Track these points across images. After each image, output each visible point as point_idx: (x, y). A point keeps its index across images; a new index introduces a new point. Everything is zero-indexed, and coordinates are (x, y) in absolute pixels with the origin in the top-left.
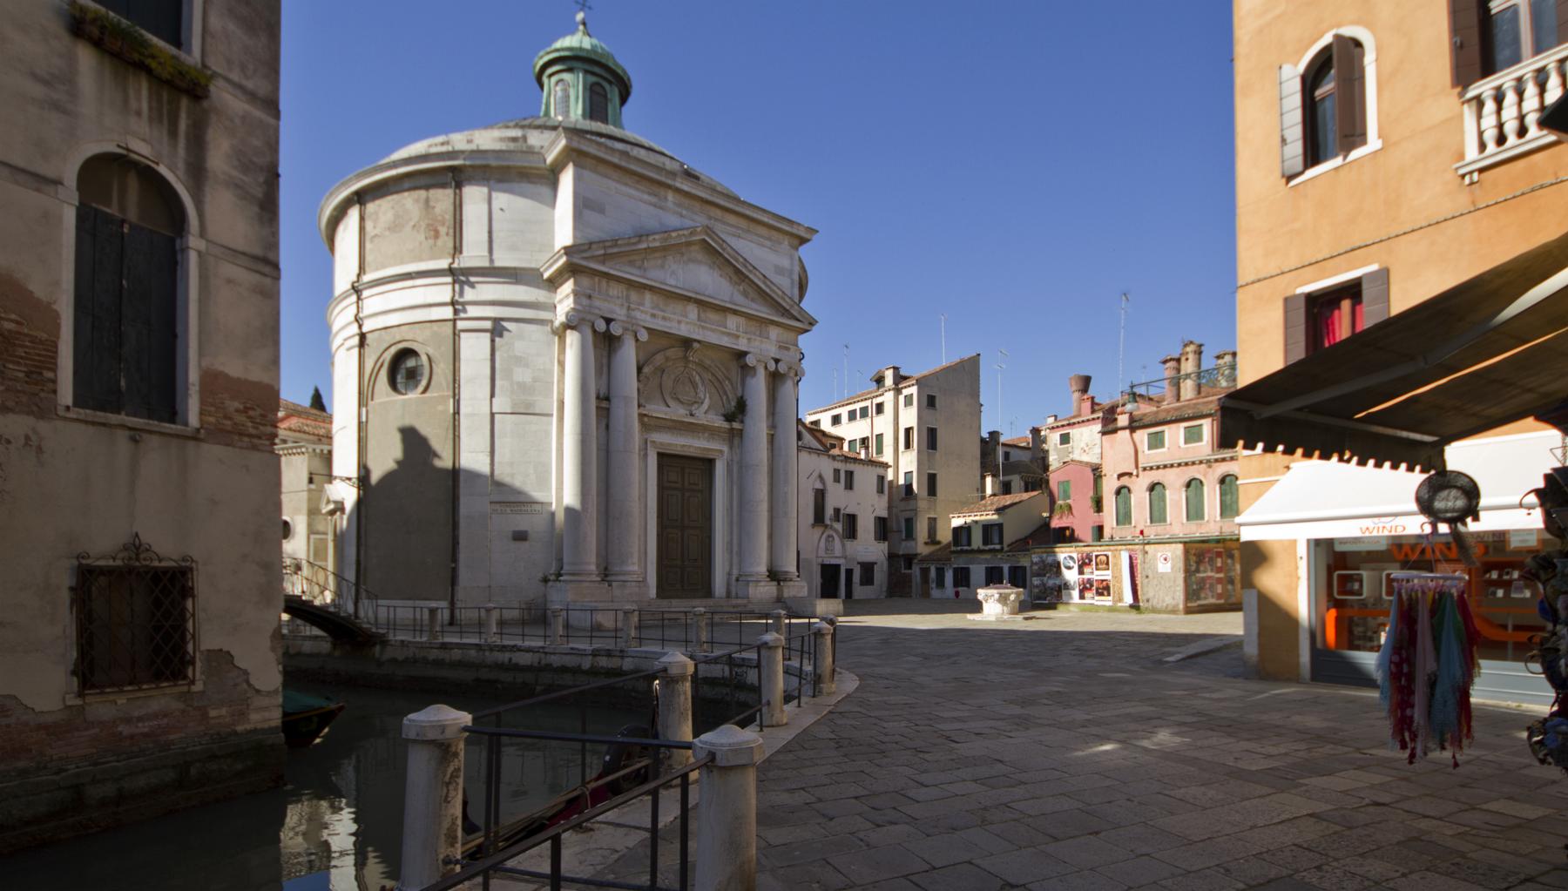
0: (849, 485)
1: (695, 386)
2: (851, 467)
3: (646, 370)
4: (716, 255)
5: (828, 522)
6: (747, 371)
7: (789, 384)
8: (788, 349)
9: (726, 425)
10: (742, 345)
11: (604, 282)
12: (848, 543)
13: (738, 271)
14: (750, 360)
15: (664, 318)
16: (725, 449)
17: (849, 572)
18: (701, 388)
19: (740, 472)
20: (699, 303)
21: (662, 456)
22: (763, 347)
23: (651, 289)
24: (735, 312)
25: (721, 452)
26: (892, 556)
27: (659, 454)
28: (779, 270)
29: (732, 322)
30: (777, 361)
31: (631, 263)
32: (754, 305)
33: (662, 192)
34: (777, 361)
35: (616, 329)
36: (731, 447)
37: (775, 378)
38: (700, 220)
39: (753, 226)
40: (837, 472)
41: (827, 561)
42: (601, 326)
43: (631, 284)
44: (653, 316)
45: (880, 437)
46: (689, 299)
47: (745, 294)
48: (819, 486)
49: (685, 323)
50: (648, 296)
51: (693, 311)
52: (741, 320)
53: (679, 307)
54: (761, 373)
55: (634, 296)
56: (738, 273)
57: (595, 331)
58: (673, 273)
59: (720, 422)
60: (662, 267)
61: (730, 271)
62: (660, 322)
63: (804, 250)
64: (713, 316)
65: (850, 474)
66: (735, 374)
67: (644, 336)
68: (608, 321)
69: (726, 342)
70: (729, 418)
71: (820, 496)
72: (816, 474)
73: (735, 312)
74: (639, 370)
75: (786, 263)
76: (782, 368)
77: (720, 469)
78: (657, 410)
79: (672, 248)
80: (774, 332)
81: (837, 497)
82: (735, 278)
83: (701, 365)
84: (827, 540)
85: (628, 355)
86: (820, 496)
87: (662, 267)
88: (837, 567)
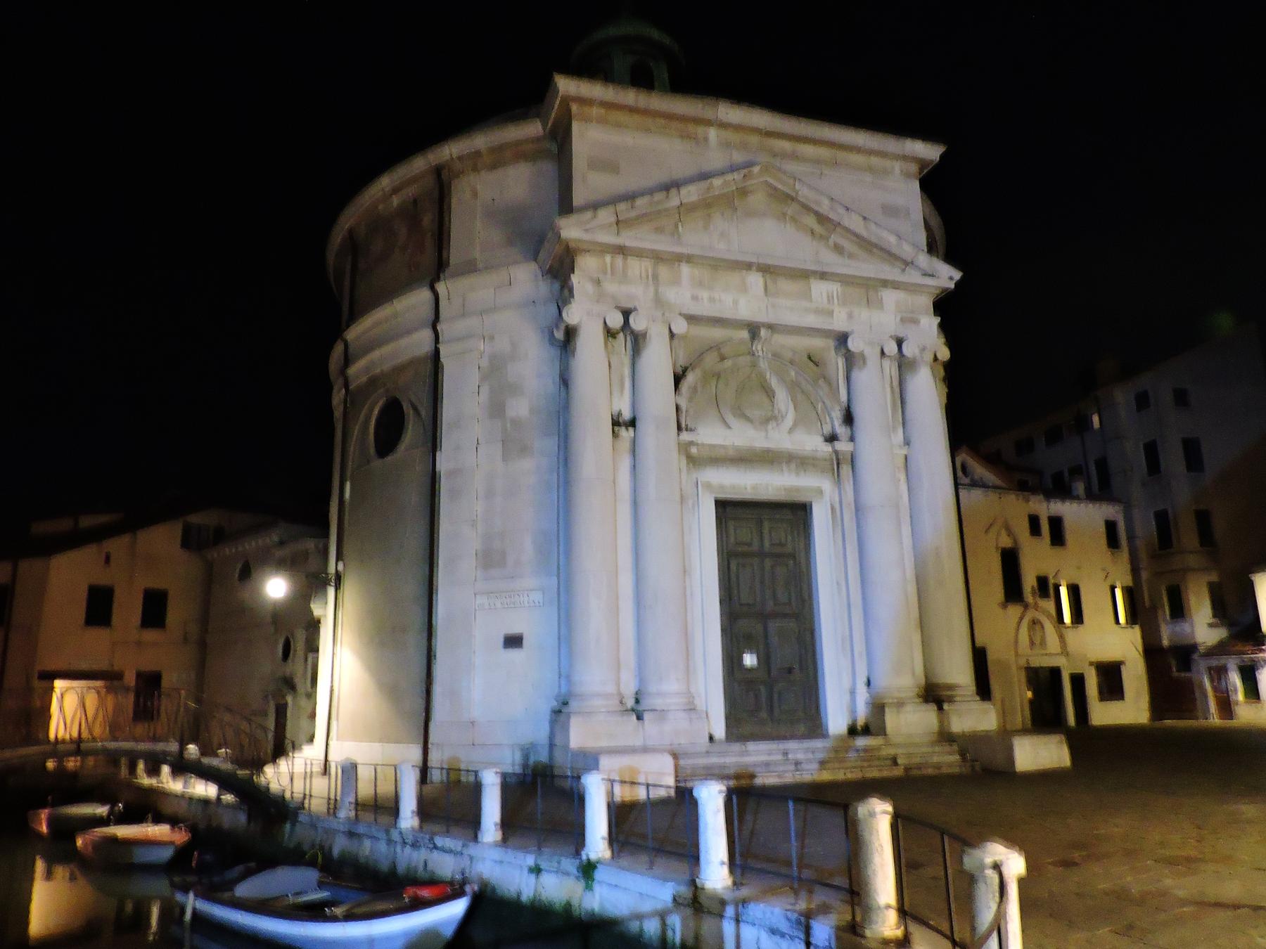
1: (770, 394)
3: (690, 378)
5: (1028, 596)
9: (827, 449)
10: (839, 323)
11: (619, 260)
13: (822, 219)
16: (826, 484)
17: (1078, 681)
18: (782, 396)
20: (765, 269)
21: (725, 507)
23: (689, 259)
24: (823, 276)
26: (1152, 652)
29: (821, 290)
31: (660, 230)
33: (700, 130)
34: (900, 343)
36: (838, 480)
39: (841, 155)
40: (1034, 523)
46: (749, 266)
47: (838, 249)
48: (1006, 542)
49: (745, 300)
50: (685, 269)
51: (755, 280)
52: (834, 288)
53: (734, 278)
55: (664, 271)
59: (812, 443)
60: (706, 228)
61: (810, 221)
65: (1056, 524)
69: (811, 321)
70: (832, 438)
71: (1010, 561)
74: (678, 379)
77: (820, 517)
78: (710, 434)
80: (890, 297)
82: (818, 229)
86: (1010, 561)
88: (1055, 673)
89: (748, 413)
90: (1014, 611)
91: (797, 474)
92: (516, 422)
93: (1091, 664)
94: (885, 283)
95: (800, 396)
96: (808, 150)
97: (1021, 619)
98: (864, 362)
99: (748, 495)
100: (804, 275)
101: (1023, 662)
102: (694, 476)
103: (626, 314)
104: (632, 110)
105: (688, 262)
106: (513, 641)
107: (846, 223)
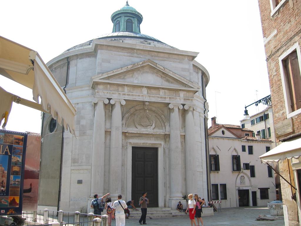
0: (251, 152)
2: (250, 144)
4: (154, 69)
6: (171, 110)
7: (190, 114)
8: (188, 99)
10: (167, 101)
11: (109, 86)
12: (252, 179)
13: (164, 73)
14: (171, 106)
15: (132, 95)
16: (163, 143)
17: (254, 193)
19: (168, 152)
22: (177, 101)
23: (127, 85)
25: (161, 144)
27: (133, 147)
28: (184, 70)
29: (162, 92)
30: (183, 105)
32: (172, 85)
34: (183, 105)
35: (112, 102)
36: (165, 142)
37: (184, 112)
38: (148, 57)
41: (241, 188)
42: (107, 102)
43: (118, 85)
44: (129, 95)
45: (269, 129)
46: (143, 87)
47: (168, 81)
48: (235, 154)
50: (126, 88)
52: (166, 91)
54: (176, 110)
56: (164, 75)
57: (104, 103)
58: (136, 78)
62: (131, 97)
63: (195, 59)
64: (153, 91)
66: (166, 111)
67: (124, 103)
68: (110, 99)
69: (159, 100)
72: (232, 149)
73: (163, 89)
75: (187, 66)
76: (186, 107)
79: (134, 70)
80: (182, 94)
81: (245, 158)
82: (163, 76)
83: (150, 110)
84: (241, 178)
85: (117, 112)
87: (132, 77)
88: (247, 191)
89: (142, 124)
90: (236, 173)
91: (155, 140)
92: (82, 126)
93: (259, 189)
94: (180, 90)
95: (157, 120)
96: (162, 55)
97: (238, 176)
98: (174, 111)
99: (141, 146)
100: (158, 88)
101: (237, 188)
102: (127, 141)
103: (110, 99)
104: (115, 47)
105: (126, 86)
106: (80, 182)
107: (169, 74)
